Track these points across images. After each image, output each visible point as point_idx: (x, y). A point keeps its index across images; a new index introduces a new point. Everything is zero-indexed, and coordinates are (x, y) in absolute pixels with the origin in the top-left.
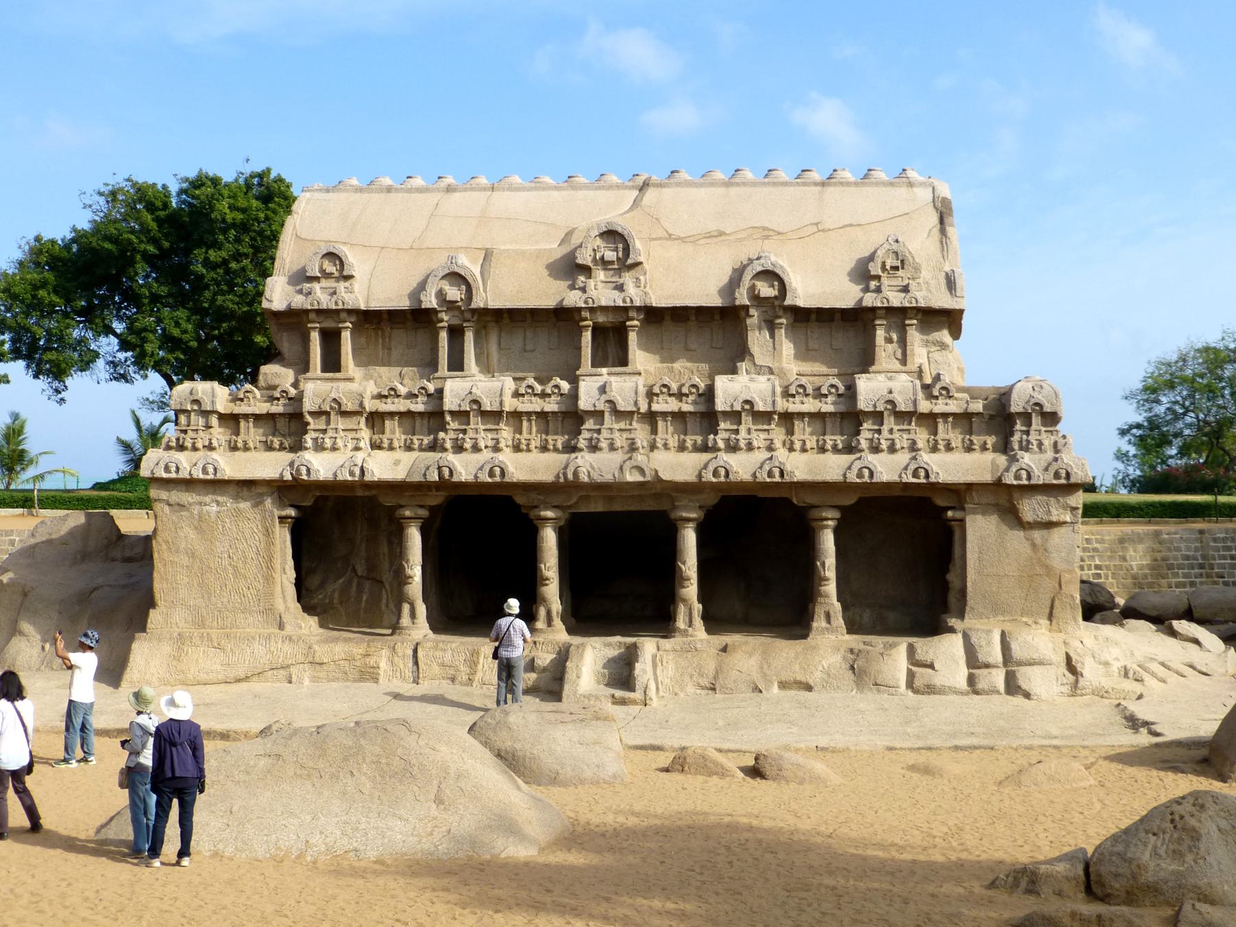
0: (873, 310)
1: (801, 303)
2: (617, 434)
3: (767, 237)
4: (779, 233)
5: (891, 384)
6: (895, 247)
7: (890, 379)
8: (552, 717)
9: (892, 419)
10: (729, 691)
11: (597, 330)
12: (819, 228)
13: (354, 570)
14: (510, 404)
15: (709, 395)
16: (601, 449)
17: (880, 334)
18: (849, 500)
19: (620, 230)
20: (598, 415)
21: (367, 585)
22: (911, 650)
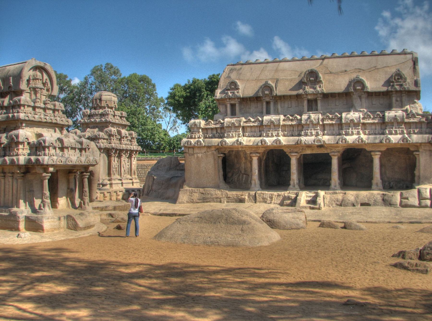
0: (392, 91)
1: (369, 90)
3: (360, 72)
4: (363, 70)
5: (396, 114)
6: (398, 72)
7: (396, 112)
8: (286, 211)
9: (396, 125)
10: (345, 206)
11: (309, 101)
12: (376, 68)
13: (241, 172)
17: (394, 99)
18: (384, 149)
21: (245, 176)
22: (401, 195)
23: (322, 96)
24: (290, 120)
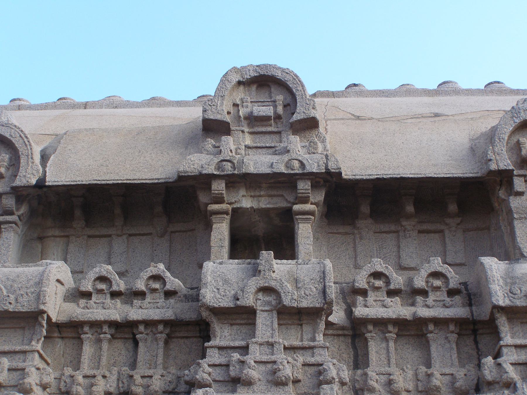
2: (280, 356)
14: (56, 308)
15: (471, 293)
16: (249, 383)
19: (279, 75)
20: (241, 315)
23: (320, 196)
24: (115, 295)
